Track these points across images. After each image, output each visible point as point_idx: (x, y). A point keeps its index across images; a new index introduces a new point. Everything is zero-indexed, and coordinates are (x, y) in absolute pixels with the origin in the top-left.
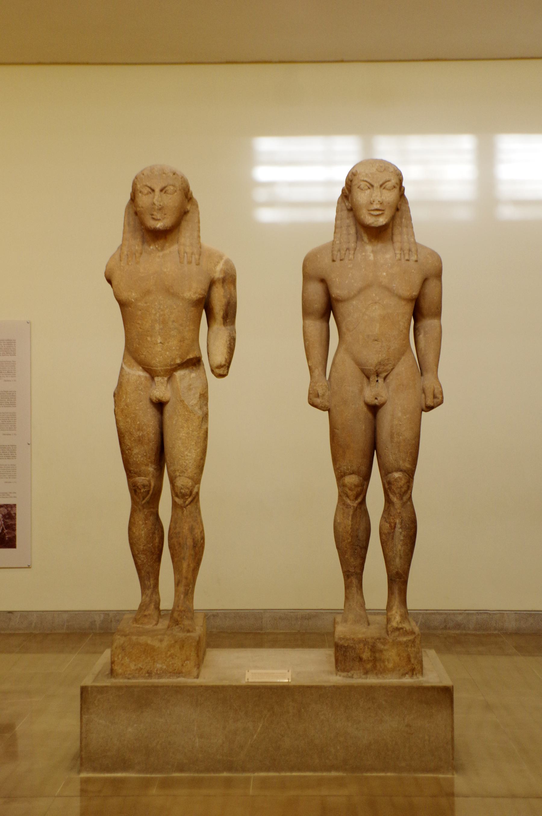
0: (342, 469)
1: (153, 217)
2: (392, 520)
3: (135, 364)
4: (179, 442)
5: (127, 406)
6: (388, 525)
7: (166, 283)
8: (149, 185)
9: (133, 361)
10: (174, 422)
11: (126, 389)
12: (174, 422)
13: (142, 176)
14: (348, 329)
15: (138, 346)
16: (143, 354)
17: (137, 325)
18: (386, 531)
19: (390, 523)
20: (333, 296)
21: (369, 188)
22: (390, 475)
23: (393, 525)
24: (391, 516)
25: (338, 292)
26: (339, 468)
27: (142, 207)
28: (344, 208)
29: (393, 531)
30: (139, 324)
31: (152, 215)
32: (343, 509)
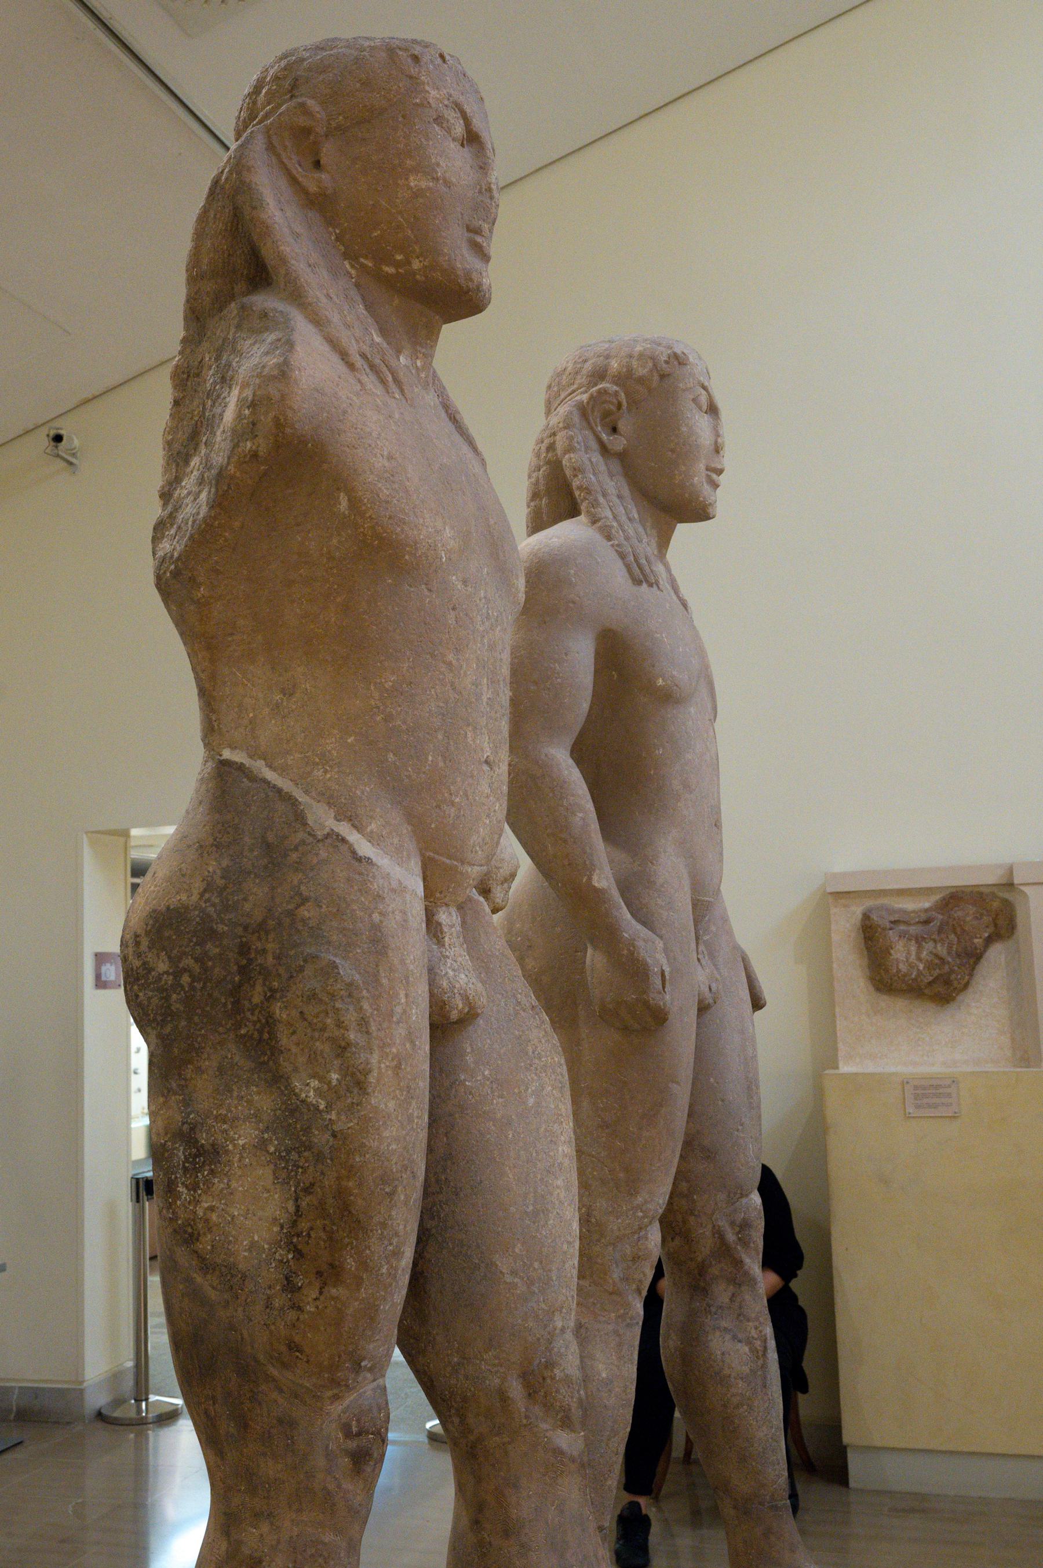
0: (649, 1206)
1: (479, 239)
2: (754, 1333)
3: (411, 845)
4: (559, 1182)
5: (413, 1043)
6: (746, 1349)
7: (492, 522)
8: (467, 109)
9: (406, 829)
10: (531, 1101)
11: (403, 962)
12: (531, 1101)
13: (439, 61)
14: (686, 786)
15: (441, 764)
16: (453, 804)
17: (443, 668)
18: (746, 1369)
19: (749, 1342)
20: (660, 682)
21: (706, 413)
22: (744, 1200)
23: (758, 1343)
24: (748, 1320)
25: (675, 673)
26: (646, 1202)
27: (447, 184)
28: (593, 444)
29: (760, 1362)
30: (450, 664)
31: (478, 231)
32: (616, 1332)
